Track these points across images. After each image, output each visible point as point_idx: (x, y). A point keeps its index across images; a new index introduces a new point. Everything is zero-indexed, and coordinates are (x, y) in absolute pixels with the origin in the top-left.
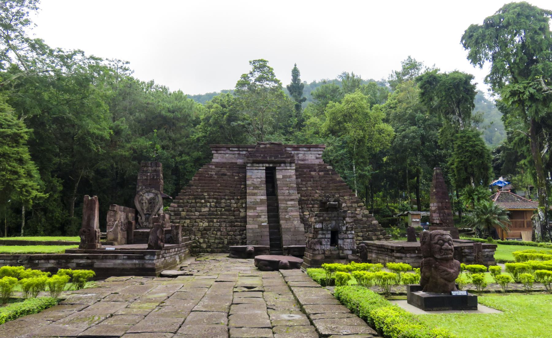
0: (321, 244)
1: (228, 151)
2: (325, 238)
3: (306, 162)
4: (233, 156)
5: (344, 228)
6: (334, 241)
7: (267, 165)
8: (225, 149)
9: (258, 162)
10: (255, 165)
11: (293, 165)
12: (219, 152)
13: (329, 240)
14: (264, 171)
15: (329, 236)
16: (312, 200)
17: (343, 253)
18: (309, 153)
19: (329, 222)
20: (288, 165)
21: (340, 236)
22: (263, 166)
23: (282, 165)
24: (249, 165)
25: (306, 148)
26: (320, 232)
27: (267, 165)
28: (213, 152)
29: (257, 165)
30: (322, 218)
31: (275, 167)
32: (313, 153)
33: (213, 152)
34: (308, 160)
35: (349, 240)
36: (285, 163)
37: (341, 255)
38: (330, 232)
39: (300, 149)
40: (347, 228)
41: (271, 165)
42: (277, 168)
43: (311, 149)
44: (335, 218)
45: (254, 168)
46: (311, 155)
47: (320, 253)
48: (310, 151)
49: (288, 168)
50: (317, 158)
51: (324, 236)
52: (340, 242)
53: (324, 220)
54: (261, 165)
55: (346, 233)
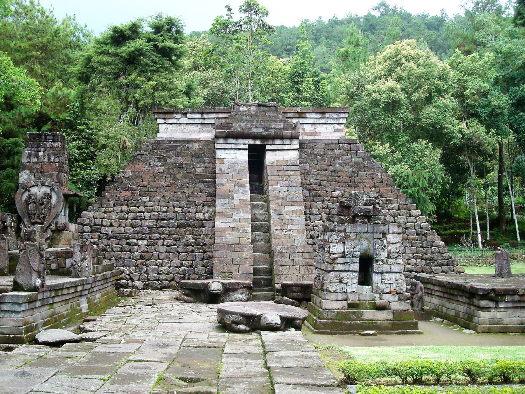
0: (341, 282)
1: (184, 120)
2: (348, 271)
3: (317, 138)
4: (192, 128)
5: (384, 254)
6: (365, 278)
7: (251, 142)
8: (179, 116)
9: (237, 136)
10: (230, 141)
11: (296, 142)
12: (171, 121)
13: (356, 275)
14: (247, 152)
15: (357, 267)
17: (381, 299)
18: (323, 121)
19: (356, 241)
20: (288, 142)
21: (376, 267)
22: (244, 144)
23: (278, 142)
26: (341, 260)
27: (251, 142)
28: (159, 121)
29: (234, 141)
30: (342, 234)
31: (264, 146)
32: (330, 121)
33: (159, 121)
34: (320, 133)
35: (393, 276)
36: (282, 138)
37: (378, 302)
38: (357, 260)
39: (308, 115)
40: (389, 253)
41: (258, 142)
42: (268, 147)
43: (327, 115)
44: (367, 235)
45: (229, 146)
46: (325, 126)
47: (340, 297)
49: (287, 147)
50: (335, 130)
51: (346, 268)
52: (376, 278)
53: (347, 237)
54: (241, 141)
55: (387, 263)
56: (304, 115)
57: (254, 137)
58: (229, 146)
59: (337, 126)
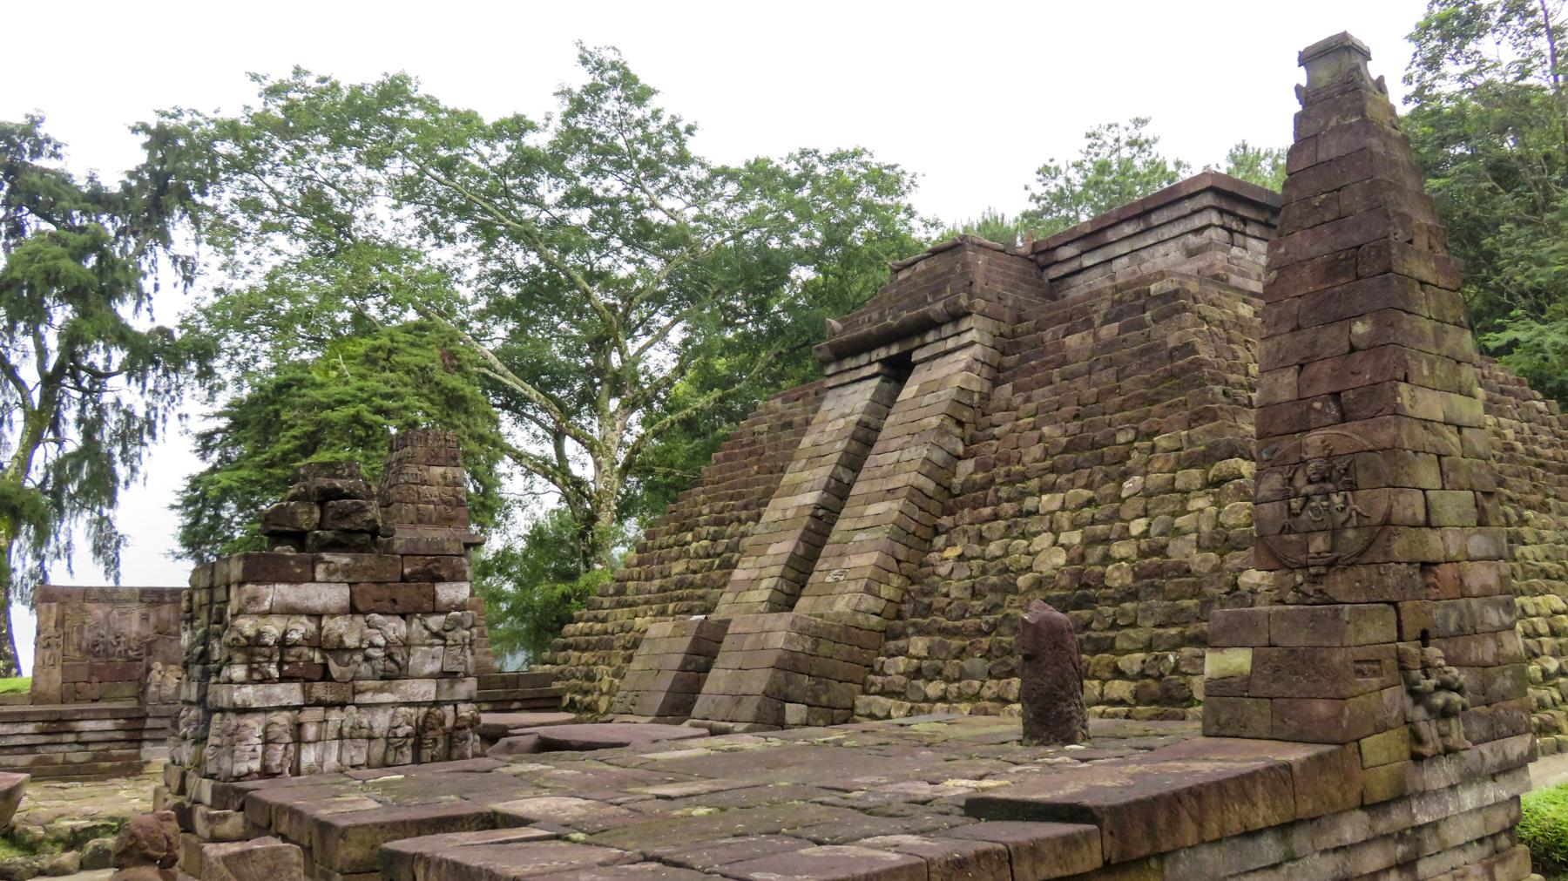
7: (882, 353)
10: (849, 363)
16: (1010, 480)
18: (1150, 239)
22: (870, 363)
24: (830, 370)
25: (1128, 220)
27: (882, 353)
31: (909, 353)
32: (1167, 232)
39: (1111, 235)
41: (895, 350)
43: (1155, 219)
46: (1161, 249)
48: (1150, 229)
49: (951, 344)
50: (1191, 253)
54: (864, 359)
56: (1101, 239)
57: (885, 338)
58: (847, 378)
59: (1193, 240)
